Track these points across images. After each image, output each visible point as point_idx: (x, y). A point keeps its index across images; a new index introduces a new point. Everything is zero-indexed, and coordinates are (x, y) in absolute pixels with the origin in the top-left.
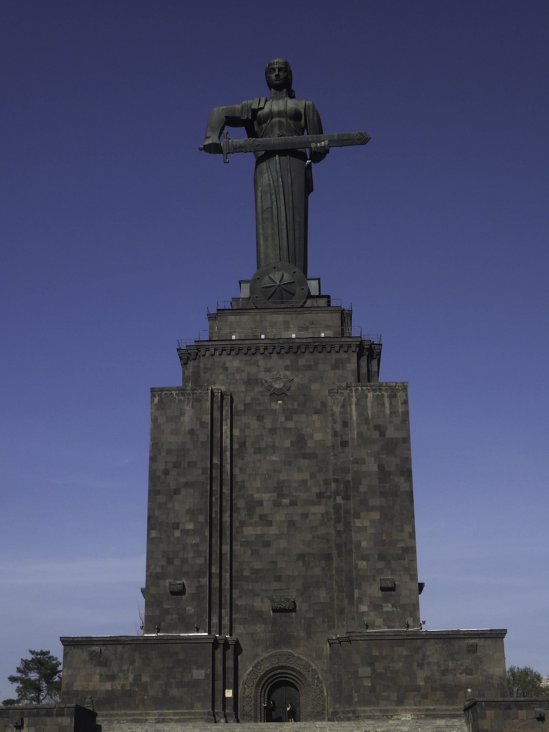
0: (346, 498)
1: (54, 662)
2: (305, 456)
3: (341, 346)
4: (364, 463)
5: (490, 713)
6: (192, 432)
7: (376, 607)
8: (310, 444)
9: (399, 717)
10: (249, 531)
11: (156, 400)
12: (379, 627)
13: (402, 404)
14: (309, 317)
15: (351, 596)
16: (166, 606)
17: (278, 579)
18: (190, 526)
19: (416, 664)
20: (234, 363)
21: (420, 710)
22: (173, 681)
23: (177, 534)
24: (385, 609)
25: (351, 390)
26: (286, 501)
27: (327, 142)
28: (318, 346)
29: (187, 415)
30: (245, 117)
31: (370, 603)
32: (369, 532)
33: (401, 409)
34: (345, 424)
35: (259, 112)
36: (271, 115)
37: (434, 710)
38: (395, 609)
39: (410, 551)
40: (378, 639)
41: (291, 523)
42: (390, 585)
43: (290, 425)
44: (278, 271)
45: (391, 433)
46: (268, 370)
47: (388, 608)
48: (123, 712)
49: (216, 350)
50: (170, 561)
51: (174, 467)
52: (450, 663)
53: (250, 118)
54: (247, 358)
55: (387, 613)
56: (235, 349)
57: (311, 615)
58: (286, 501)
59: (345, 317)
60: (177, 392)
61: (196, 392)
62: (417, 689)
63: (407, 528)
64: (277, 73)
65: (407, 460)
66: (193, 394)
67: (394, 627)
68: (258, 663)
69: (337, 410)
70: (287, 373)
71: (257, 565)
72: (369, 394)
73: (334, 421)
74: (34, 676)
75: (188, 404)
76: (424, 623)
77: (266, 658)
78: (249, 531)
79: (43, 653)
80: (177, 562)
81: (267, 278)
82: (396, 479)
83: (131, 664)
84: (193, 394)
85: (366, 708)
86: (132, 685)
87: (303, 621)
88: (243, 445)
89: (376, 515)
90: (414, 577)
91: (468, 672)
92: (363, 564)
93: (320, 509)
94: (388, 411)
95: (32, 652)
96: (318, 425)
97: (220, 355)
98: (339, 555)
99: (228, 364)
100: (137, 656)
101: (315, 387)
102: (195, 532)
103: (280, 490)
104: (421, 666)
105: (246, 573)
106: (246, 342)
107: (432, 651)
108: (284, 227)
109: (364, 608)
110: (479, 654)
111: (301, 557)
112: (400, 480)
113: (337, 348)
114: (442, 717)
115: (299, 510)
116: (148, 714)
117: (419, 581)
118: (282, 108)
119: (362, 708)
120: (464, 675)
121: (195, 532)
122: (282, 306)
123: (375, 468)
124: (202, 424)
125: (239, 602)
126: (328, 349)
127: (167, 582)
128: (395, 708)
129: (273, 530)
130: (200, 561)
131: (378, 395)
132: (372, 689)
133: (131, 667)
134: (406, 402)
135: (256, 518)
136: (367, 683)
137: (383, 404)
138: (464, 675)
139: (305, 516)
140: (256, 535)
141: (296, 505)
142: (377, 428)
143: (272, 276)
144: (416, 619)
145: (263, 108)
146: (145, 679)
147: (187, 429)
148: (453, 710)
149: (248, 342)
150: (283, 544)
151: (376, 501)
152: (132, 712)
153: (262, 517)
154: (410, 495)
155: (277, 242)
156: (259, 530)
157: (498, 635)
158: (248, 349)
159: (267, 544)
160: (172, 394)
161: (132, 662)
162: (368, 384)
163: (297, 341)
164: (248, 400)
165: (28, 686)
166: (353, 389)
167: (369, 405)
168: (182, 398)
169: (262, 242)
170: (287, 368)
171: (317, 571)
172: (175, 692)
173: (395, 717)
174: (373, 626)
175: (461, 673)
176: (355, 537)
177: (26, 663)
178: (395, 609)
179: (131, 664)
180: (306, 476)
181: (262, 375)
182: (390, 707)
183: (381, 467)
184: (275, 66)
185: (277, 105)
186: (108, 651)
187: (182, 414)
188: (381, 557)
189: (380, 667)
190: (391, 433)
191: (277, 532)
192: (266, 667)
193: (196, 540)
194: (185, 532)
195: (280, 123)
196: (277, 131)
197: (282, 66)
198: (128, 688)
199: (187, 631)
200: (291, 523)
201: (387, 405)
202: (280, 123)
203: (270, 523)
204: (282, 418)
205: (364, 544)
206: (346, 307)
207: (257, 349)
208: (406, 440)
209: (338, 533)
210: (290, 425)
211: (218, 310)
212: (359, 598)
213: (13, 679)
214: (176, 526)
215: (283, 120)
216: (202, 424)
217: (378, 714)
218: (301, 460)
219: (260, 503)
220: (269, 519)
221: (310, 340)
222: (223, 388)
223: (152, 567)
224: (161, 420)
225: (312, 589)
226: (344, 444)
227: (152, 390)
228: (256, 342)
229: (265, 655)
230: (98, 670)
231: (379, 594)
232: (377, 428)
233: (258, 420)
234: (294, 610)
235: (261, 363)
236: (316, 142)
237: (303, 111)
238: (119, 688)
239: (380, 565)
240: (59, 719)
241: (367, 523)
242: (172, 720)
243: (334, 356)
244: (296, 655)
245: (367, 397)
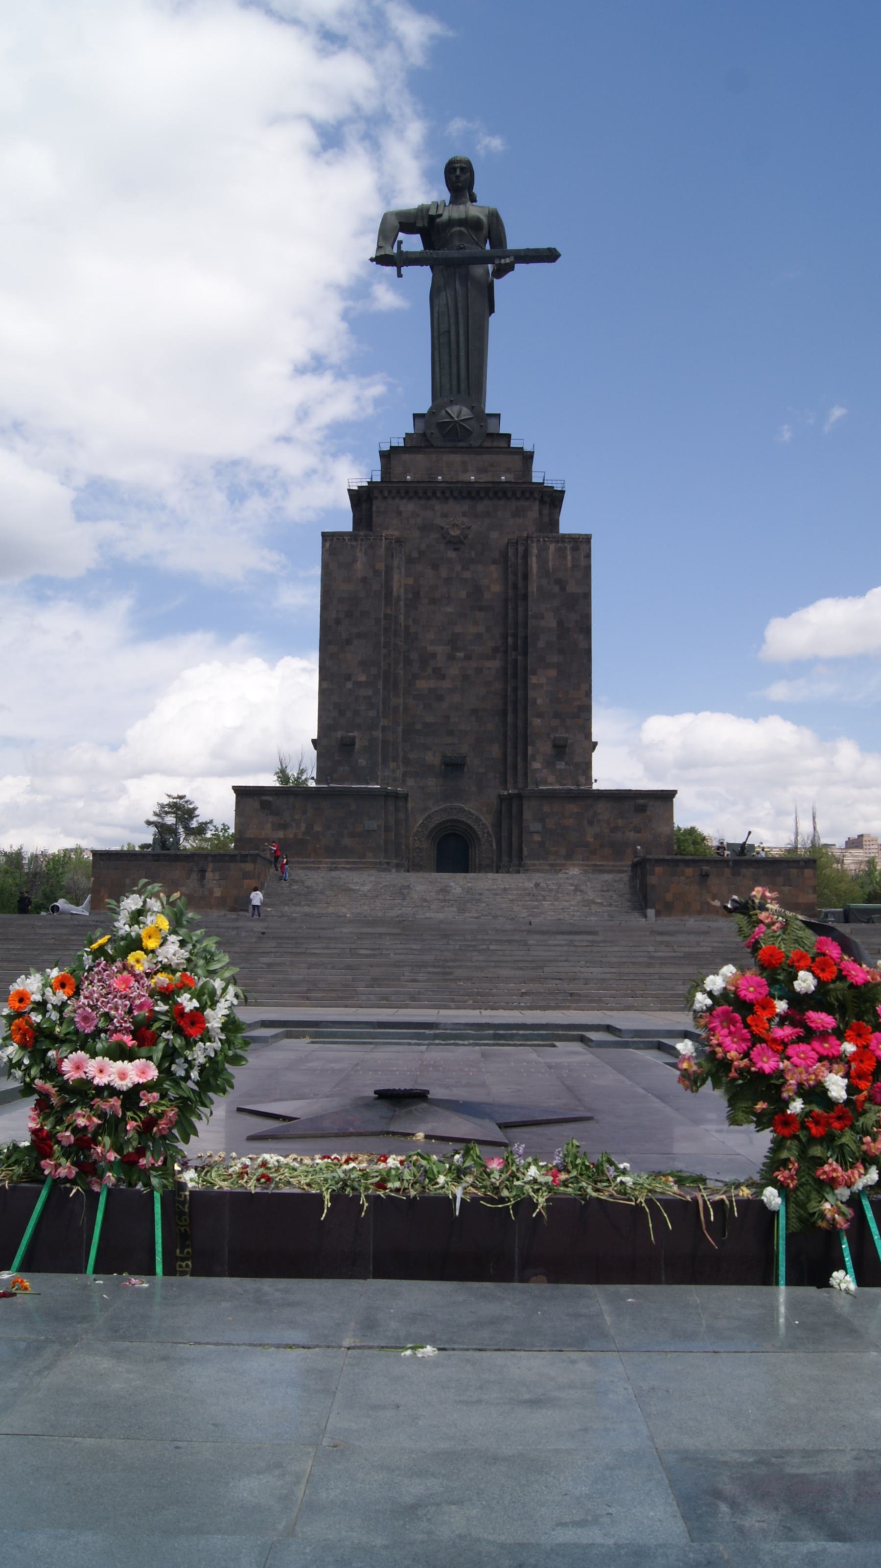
1: (191, 806)
2: (481, 609)
3: (523, 493)
5: (658, 870)
6: (364, 580)
7: (549, 764)
10: (422, 685)
11: (328, 544)
12: (551, 784)
14: (488, 458)
17: (451, 733)
18: (362, 678)
20: (409, 507)
21: (587, 866)
23: (349, 685)
26: (460, 655)
27: (512, 259)
28: (497, 492)
29: (359, 563)
30: (420, 224)
33: (582, 562)
34: (526, 577)
35: (438, 220)
36: (451, 223)
37: (602, 865)
40: (551, 796)
43: (467, 575)
44: (456, 404)
45: (572, 588)
46: (445, 515)
47: (561, 765)
48: (296, 859)
49: (390, 492)
52: (620, 821)
53: (426, 225)
54: (423, 502)
56: (410, 492)
57: (482, 770)
59: (527, 457)
64: (458, 172)
68: (429, 817)
70: (465, 519)
71: (430, 719)
74: (170, 820)
75: (361, 550)
76: (596, 781)
77: (436, 811)
78: (422, 685)
79: (181, 797)
81: (443, 412)
85: (537, 862)
88: (417, 595)
89: (553, 673)
90: (589, 734)
91: (637, 830)
94: (569, 564)
95: (169, 796)
97: (394, 498)
98: (515, 711)
99: (402, 508)
101: (494, 535)
104: (591, 823)
105: (418, 727)
106: (421, 485)
107: (603, 809)
108: (462, 354)
110: (648, 813)
111: (475, 712)
113: (518, 494)
114: (610, 872)
116: (320, 862)
117: (594, 740)
118: (463, 216)
119: (532, 862)
123: (554, 624)
125: (412, 756)
127: (339, 734)
128: (564, 862)
129: (446, 684)
130: (372, 713)
131: (560, 547)
134: (588, 556)
137: (565, 558)
139: (479, 670)
142: (558, 582)
143: (449, 411)
145: (441, 215)
146: (318, 828)
149: (424, 485)
151: (555, 658)
152: (305, 860)
154: (588, 652)
155: (454, 370)
156: (432, 684)
157: (668, 797)
158: (423, 492)
159: (440, 698)
162: (550, 535)
163: (476, 485)
164: (423, 547)
165: (163, 830)
166: (535, 540)
167: (550, 557)
168: (354, 543)
169: (437, 370)
170: (464, 514)
172: (346, 841)
174: (545, 783)
175: (630, 831)
176: (531, 694)
177: (162, 806)
181: (439, 521)
182: (559, 862)
183: (560, 623)
184: (456, 165)
185: (458, 212)
187: (355, 561)
188: (557, 715)
190: (572, 588)
192: (437, 820)
193: (370, 692)
194: (358, 684)
195: (461, 233)
196: (457, 243)
197: (464, 165)
198: (300, 836)
201: (569, 558)
203: (443, 677)
204: (458, 568)
205: (539, 701)
206: (527, 448)
207: (434, 493)
208: (587, 596)
209: (515, 690)
210: (467, 575)
211: (391, 447)
213: (149, 823)
214: (348, 677)
215: (463, 229)
216: (376, 572)
219: (434, 656)
221: (490, 485)
222: (397, 533)
227: (324, 535)
228: (433, 485)
229: (436, 809)
232: (558, 582)
236: (500, 258)
237: (484, 219)
238: (291, 836)
239: (555, 722)
240: (243, 866)
241: (543, 680)
242: (344, 868)
244: (467, 809)
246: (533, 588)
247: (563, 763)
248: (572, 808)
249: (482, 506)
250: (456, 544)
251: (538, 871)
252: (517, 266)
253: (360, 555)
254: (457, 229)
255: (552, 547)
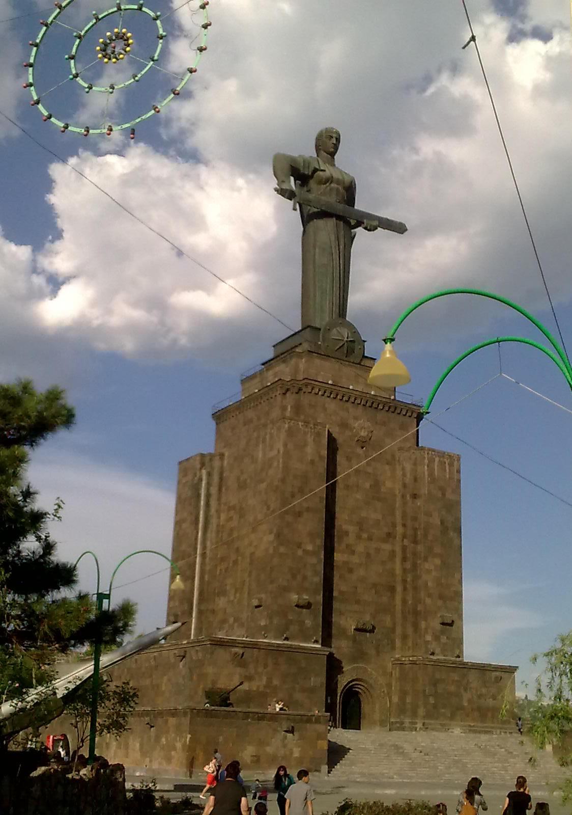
0: (415, 542)
2: (379, 499)
4: (431, 516)
7: (437, 638)
8: (383, 489)
9: (453, 730)
12: (438, 655)
13: (457, 472)
15: (416, 626)
16: (290, 618)
17: (358, 602)
18: (310, 547)
19: (463, 687)
20: (332, 405)
22: (297, 686)
25: (424, 452)
29: (309, 447)
31: (433, 633)
32: (434, 573)
35: (321, 173)
37: (474, 726)
38: (448, 641)
39: (458, 595)
41: (368, 555)
42: (449, 621)
45: (449, 495)
47: (444, 639)
50: (294, 576)
51: (299, 492)
53: (310, 174)
55: (445, 644)
58: (365, 536)
60: (303, 424)
61: (316, 427)
62: (462, 708)
63: (457, 576)
65: (458, 520)
66: (315, 428)
67: (447, 656)
69: (408, 467)
71: (344, 588)
72: (436, 459)
73: (404, 475)
80: (299, 578)
82: (451, 534)
83: (265, 668)
84: (315, 428)
85: (432, 722)
86: (265, 687)
91: (494, 698)
92: (428, 601)
93: (387, 547)
96: (389, 474)
99: (327, 405)
100: (270, 661)
102: (314, 553)
103: (361, 524)
104: (466, 690)
109: (429, 638)
111: (374, 585)
112: (452, 534)
120: (491, 700)
121: (314, 553)
122: (346, 359)
124: (321, 457)
126: (398, 411)
129: (355, 559)
132: (435, 706)
133: (265, 670)
134: (459, 472)
135: (343, 546)
136: (432, 700)
137: (445, 471)
138: (491, 700)
140: (343, 561)
141: (371, 540)
144: (462, 651)
146: (276, 682)
147: (309, 459)
148: (486, 727)
150: (362, 572)
151: (438, 550)
153: (348, 546)
159: (351, 571)
160: (298, 424)
161: (266, 666)
171: (385, 599)
173: (450, 730)
175: (489, 698)
176: (425, 577)
179: (265, 668)
180: (380, 517)
181: (351, 421)
183: (442, 522)
186: (248, 653)
187: (306, 445)
188: (441, 597)
189: (440, 688)
191: (357, 561)
195: (337, 189)
198: (261, 689)
199: (306, 641)
200: (368, 555)
201: (448, 471)
202: (337, 189)
205: (430, 584)
208: (458, 503)
214: (299, 546)
216: (321, 457)
217: (440, 727)
218: (377, 502)
219: (347, 533)
220: (353, 548)
221: (387, 400)
223: (280, 580)
224: (290, 446)
226: (415, 496)
230: (239, 670)
231: (439, 627)
233: (347, 459)
234: (372, 631)
235: (350, 410)
239: (440, 603)
243: (401, 418)
245: (435, 461)
246: (424, 491)
247: (445, 638)
248: (455, 676)
249: (381, 416)
250: (363, 443)
251: (433, 729)
252: (379, 229)
253: (310, 439)
254: (336, 185)
255: (437, 459)
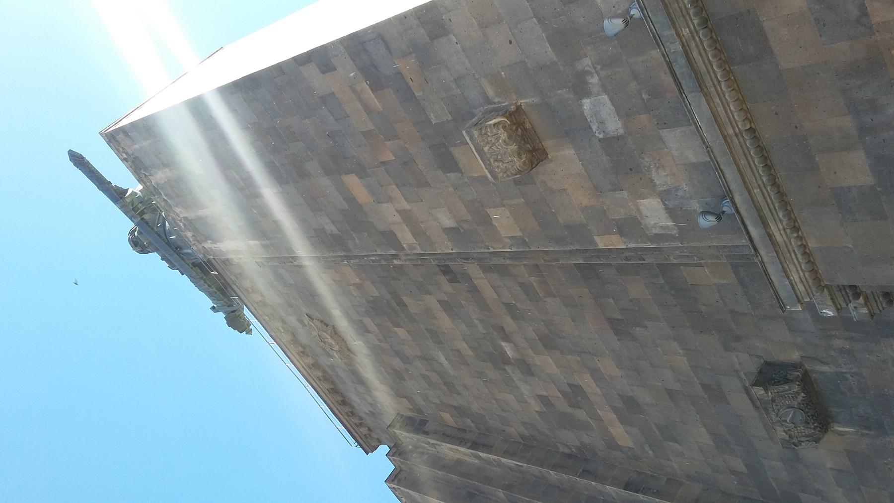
8: (373, 291)
24: (614, 126)
26: (509, 350)
32: (407, 207)
38: (594, 80)
87: (838, 343)
111: (619, 327)
115: (509, 323)
178: (594, 80)
180: (432, 302)
212: (621, 233)
225: (703, 308)
247: (587, 103)
